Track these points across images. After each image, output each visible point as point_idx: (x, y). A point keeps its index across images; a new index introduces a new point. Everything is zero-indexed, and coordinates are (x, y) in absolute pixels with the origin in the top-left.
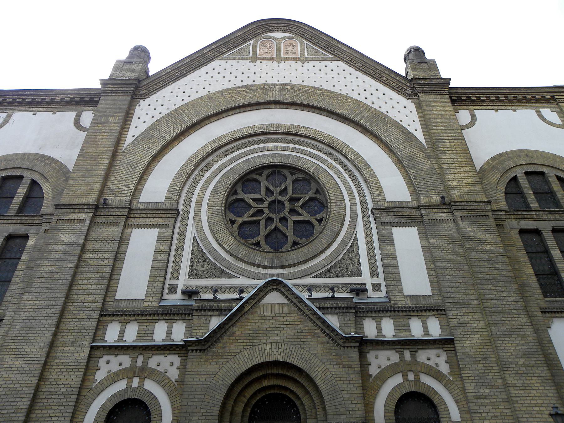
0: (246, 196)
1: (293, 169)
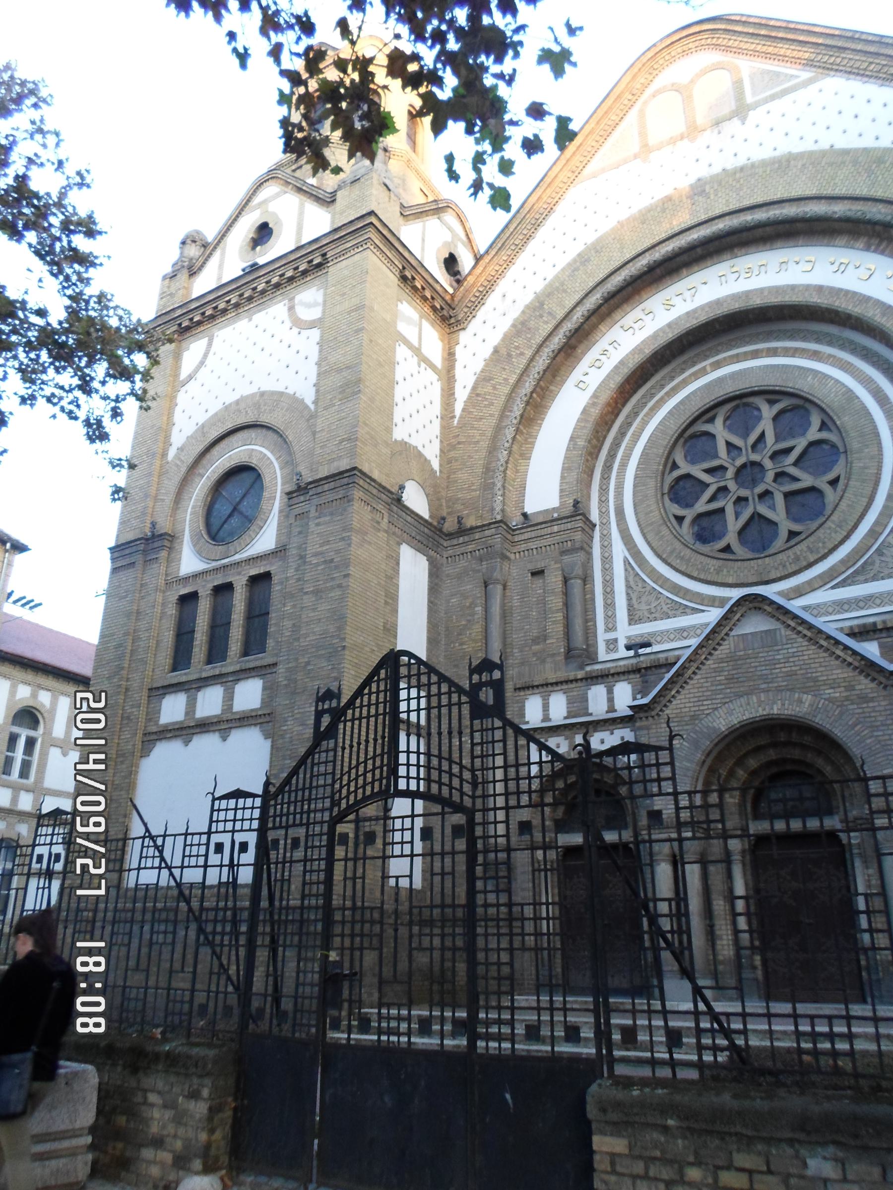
1: (772, 395)
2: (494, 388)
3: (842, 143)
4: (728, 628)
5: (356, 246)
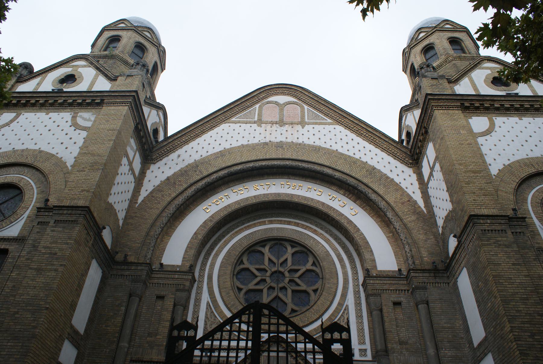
0: (252, 266)
1: (294, 243)
2: (163, 196)
3: (340, 150)
5: (122, 103)
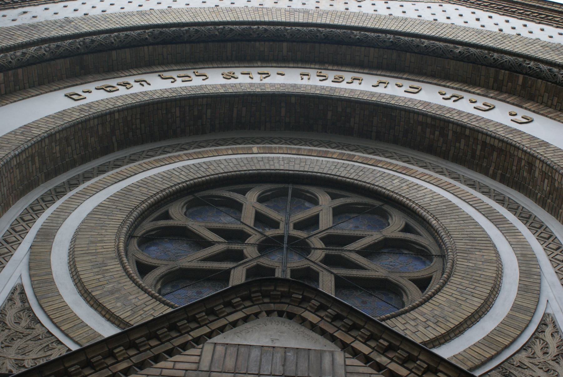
4: (205, 330)
